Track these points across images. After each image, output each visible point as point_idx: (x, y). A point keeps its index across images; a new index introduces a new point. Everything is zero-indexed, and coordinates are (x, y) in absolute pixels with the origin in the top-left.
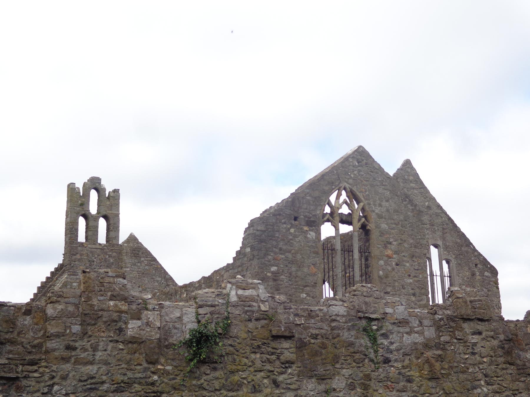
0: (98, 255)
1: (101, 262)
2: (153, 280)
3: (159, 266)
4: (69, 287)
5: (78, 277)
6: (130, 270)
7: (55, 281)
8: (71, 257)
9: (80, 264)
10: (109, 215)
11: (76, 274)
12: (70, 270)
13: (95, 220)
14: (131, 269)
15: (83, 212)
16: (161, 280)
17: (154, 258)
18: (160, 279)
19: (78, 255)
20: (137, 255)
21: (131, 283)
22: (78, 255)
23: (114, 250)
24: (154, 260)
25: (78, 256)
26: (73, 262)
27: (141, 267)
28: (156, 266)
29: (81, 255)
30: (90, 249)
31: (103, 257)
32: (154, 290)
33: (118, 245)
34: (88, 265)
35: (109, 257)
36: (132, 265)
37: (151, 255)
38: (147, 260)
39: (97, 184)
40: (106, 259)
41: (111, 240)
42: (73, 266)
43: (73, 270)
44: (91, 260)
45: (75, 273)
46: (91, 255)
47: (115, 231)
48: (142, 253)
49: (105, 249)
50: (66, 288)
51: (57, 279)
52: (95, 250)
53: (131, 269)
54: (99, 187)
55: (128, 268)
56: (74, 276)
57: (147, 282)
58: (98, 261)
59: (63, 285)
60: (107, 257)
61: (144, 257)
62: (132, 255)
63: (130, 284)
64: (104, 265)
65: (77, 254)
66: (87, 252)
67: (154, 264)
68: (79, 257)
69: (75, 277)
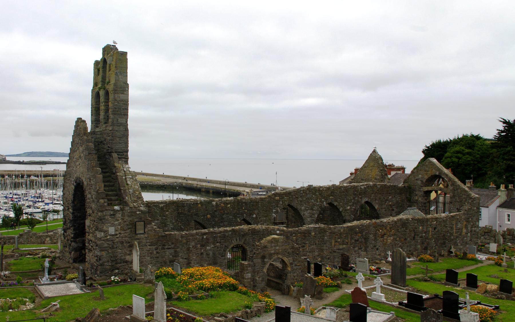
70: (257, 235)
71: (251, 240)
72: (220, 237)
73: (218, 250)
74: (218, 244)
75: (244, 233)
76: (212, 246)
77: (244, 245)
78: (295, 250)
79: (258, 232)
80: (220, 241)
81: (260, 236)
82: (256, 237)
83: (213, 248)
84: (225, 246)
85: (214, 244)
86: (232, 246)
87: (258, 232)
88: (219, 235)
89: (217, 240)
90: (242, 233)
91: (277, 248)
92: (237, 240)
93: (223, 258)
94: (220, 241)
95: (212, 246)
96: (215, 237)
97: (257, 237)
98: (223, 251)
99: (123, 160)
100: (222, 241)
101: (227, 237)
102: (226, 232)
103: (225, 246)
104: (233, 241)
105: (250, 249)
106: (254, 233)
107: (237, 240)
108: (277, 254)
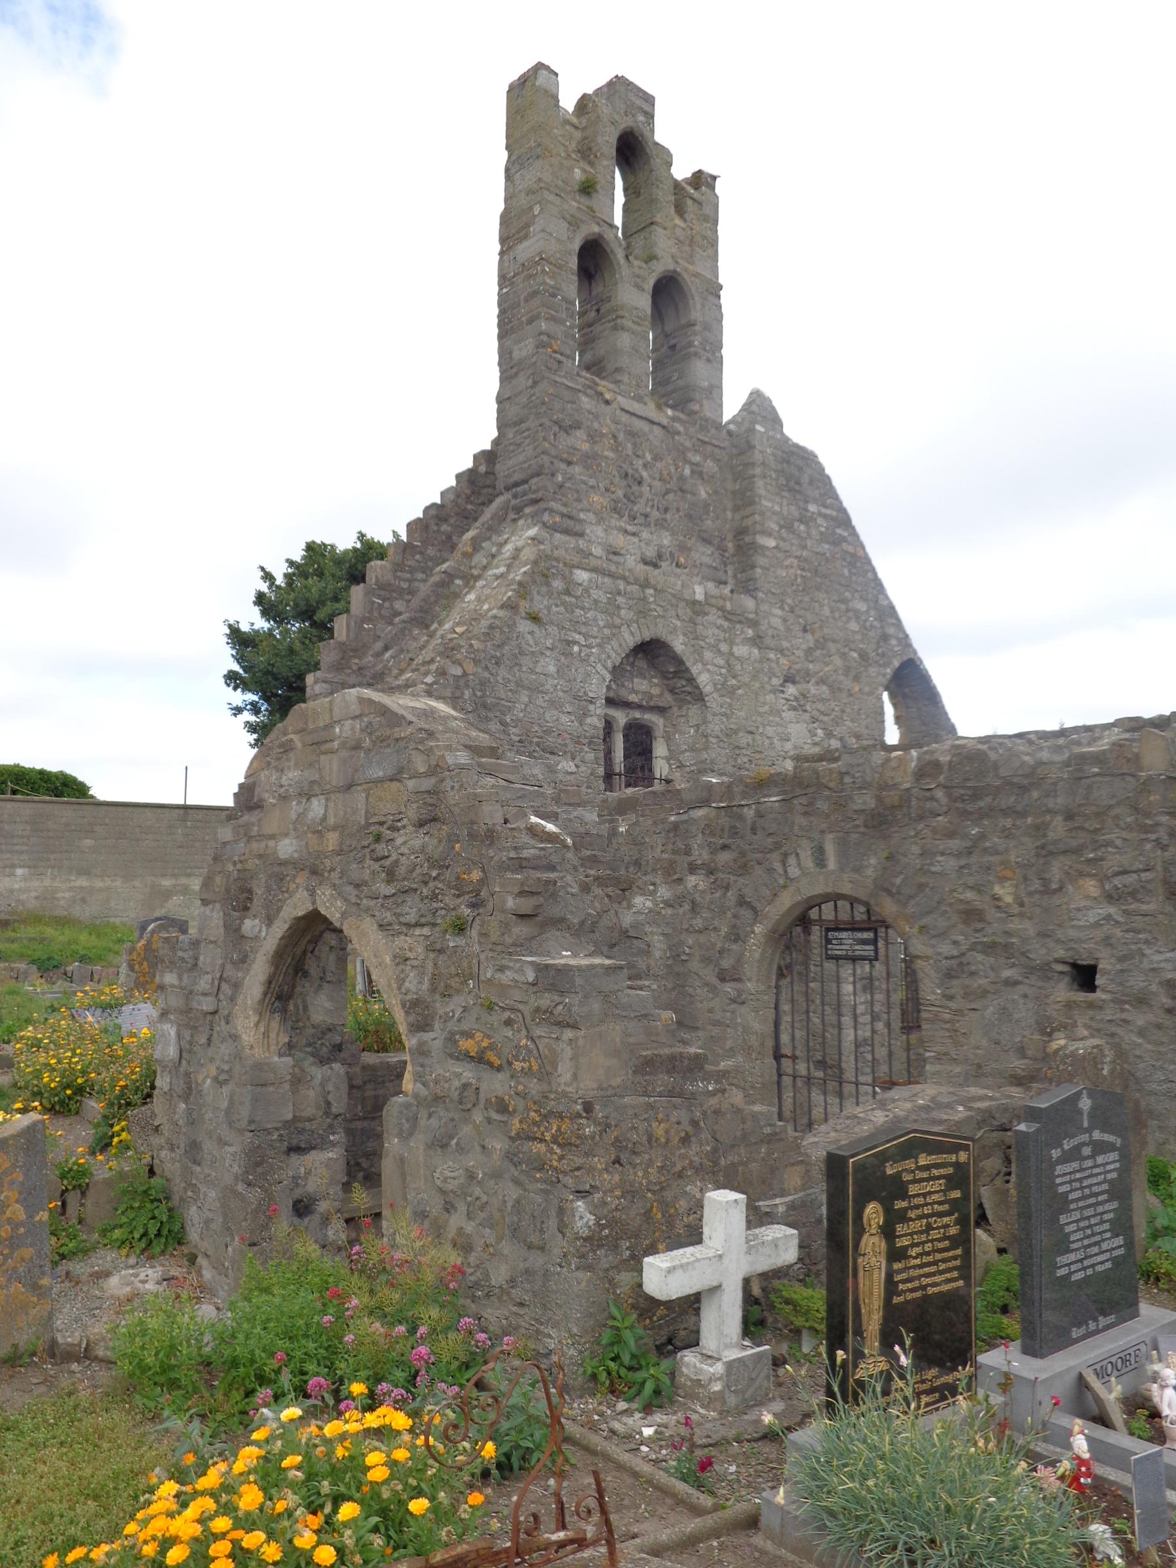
0: (657, 458)
1: (667, 492)
2: (843, 607)
3: (861, 553)
4: (558, 584)
5: (581, 543)
6: (776, 547)
7: (468, 556)
8: (555, 435)
9: (592, 482)
10: (686, 276)
11: (578, 528)
12: (552, 504)
13: (639, 280)
14: (782, 544)
15: (596, 229)
16: (867, 611)
17: (843, 511)
18: (862, 606)
19: (578, 433)
20: (797, 487)
21: (782, 608)
22: (580, 434)
23: (709, 448)
24: (843, 519)
25: (579, 441)
26: (563, 466)
27: (809, 543)
28: (851, 549)
29: (593, 437)
30: (625, 418)
31: (672, 469)
32: (847, 650)
33: (719, 426)
34: (620, 493)
35: (693, 472)
36: (781, 527)
37: (836, 497)
38: (825, 516)
39: (641, 118)
40: (682, 478)
41: (697, 396)
42: (561, 486)
43: (565, 505)
44: (630, 472)
45: (570, 523)
46: (629, 446)
47: (709, 360)
48: (811, 482)
49: (678, 433)
50: (544, 589)
51: (476, 544)
52: (644, 426)
53: (782, 544)
54: (647, 133)
55: (770, 535)
56: (568, 538)
57: (826, 611)
58: (657, 484)
59: (532, 573)
60: (687, 472)
61: (815, 501)
62: (782, 481)
63: (779, 612)
64: (678, 510)
65: (577, 426)
66: (613, 427)
67: (844, 539)
68: (585, 447)
69: (572, 542)
70: (1008, 822)
71: (952, 864)
72: (709, 829)
73: (698, 923)
74: (692, 880)
75: (879, 799)
76: (664, 892)
77: (872, 902)
78: (452, 839)
79: (1024, 789)
80: (706, 856)
81: (1040, 829)
82: (995, 840)
83: (668, 904)
84: (742, 902)
85: (670, 872)
86: (786, 901)
87: (1024, 789)
88: (699, 813)
89: (688, 852)
90: (865, 801)
91: (317, 808)
92: (821, 862)
93: (729, 988)
94: (706, 856)
95: (664, 892)
96: (676, 827)
97: (1007, 834)
98: (727, 938)
99: (527, 510)
100: (724, 857)
101: (754, 830)
102: (744, 795)
103: (742, 902)
104: (792, 860)
105: (946, 949)
106: (976, 795)
107: (821, 862)
108: (314, 872)
